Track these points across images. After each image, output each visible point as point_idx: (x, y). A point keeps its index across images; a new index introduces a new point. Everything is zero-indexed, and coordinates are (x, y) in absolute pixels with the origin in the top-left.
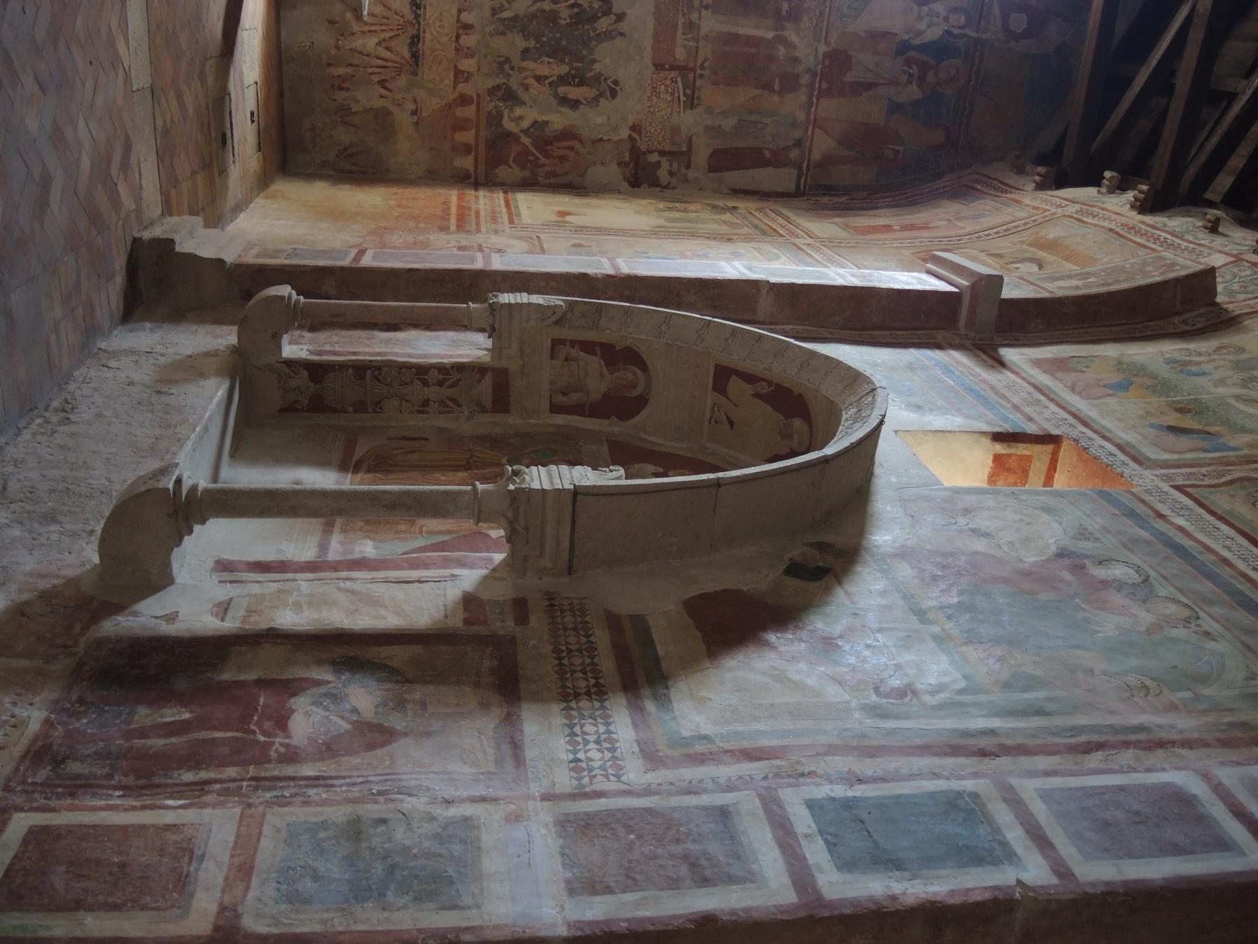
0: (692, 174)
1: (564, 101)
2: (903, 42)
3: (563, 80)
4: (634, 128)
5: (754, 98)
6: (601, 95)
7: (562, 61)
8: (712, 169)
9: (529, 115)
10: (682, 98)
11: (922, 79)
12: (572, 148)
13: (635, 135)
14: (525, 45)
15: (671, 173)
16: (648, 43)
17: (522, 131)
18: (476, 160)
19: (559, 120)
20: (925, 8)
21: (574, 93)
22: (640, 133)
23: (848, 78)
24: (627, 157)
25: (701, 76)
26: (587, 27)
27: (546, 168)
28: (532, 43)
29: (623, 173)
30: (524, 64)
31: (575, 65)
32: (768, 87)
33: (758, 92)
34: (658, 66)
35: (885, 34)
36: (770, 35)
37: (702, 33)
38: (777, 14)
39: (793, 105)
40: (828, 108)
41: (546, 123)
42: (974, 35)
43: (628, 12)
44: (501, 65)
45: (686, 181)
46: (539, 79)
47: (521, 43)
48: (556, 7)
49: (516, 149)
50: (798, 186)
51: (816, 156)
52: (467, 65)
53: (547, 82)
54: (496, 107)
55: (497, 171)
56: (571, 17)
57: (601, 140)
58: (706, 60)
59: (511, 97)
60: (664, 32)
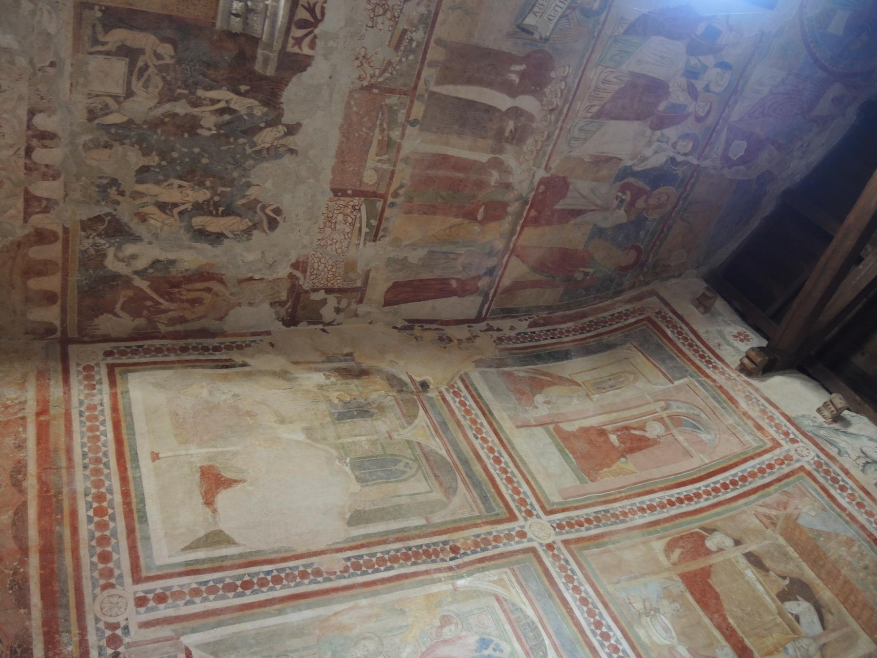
0: (362, 309)
1: (202, 234)
2: (626, 168)
3: (200, 208)
4: (296, 266)
5: (451, 227)
6: (255, 226)
7: (201, 184)
8: (387, 303)
9: (144, 253)
10: (365, 230)
11: (632, 204)
12: (209, 290)
13: (298, 274)
14: (144, 161)
15: (338, 310)
16: (328, 163)
17: (136, 273)
18: (64, 310)
19: (191, 257)
20: (658, 133)
21: (214, 224)
22: (304, 271)
23: (557, 207)
24: (284, 296)
25: (392, 205)
26: (242, 141)
27: (170, 314)
28: (154, 160)
29: (277, 313)
30: (140, 188)
31: (220, 189)
32: (471, 215)
33: (458, 220)
34: (339, 192)
35: (608, 160)
36: (484, 158)
37: (403, 153)
38: (499, 136)
39: (494, 235)
40: (531, 237)
41: (172, 262)
42: (695, 162)
43: (305, 122)
44: (103, 190)
45: (356, 315)
46: (163, 207)
47: (135, 159)
48: (195, 111)
49: (123, 296)
50: (480, 312)
51: (506, 282)
52: (44, 189)
53: (176, 211)
54: (94, 244)
55: (96, 321)
56: (219, 126)
57: (251, 279)
58: (401, 186)
59: (117, 231)
60: (351, 151)
